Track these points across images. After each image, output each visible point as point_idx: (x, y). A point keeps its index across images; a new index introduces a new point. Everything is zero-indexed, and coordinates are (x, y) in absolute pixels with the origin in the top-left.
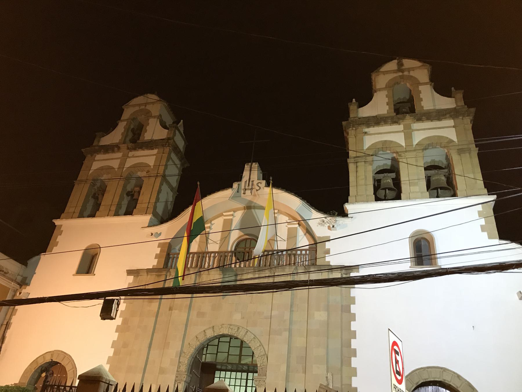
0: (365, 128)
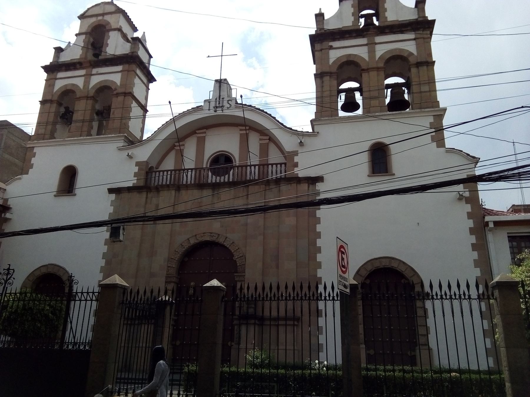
0: (330, 42)
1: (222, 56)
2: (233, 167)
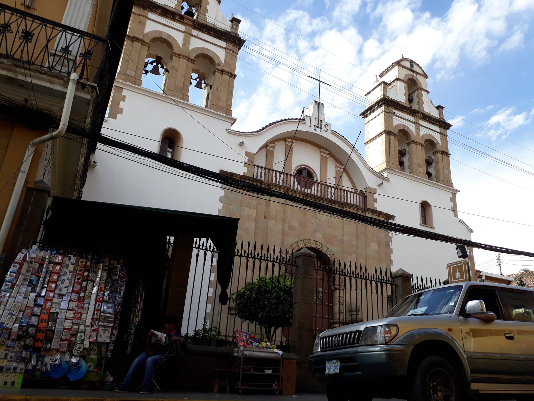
1: (320, 81)
2: (315, 182)
